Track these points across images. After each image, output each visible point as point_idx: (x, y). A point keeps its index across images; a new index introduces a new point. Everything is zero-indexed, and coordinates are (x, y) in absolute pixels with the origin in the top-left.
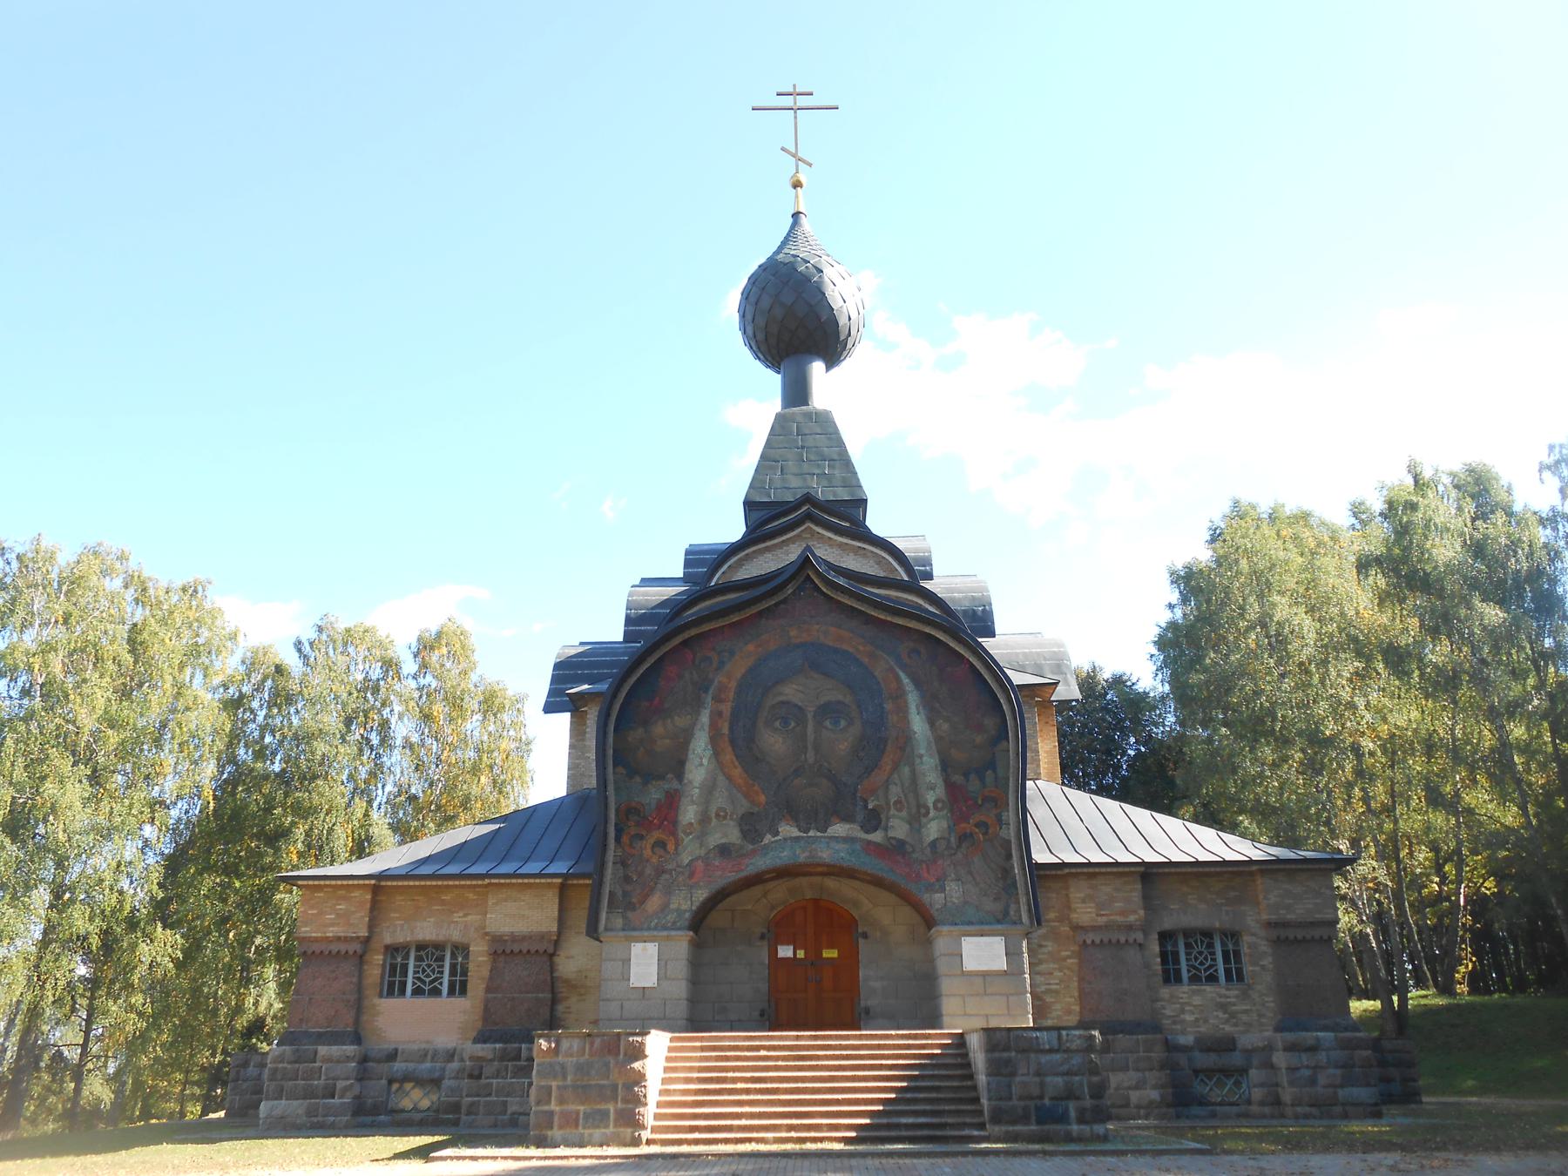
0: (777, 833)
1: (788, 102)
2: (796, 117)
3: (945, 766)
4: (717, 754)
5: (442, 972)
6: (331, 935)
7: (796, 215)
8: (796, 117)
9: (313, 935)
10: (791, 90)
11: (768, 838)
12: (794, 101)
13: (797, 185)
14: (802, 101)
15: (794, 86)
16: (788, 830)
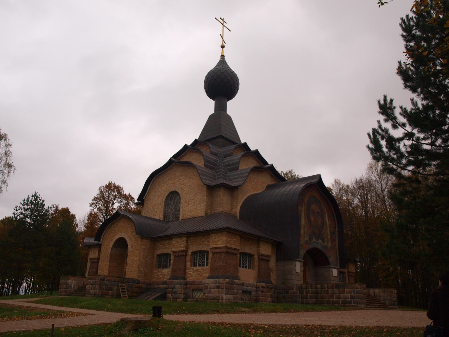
0: (313, 240)
1: (222, 21)
2: (223, 27)
3: (330, 231)
4: (305, 218)
5: (247, 262)
6: (233, 247)
7: (223, 56)
8: (223, 27)
9: (230, 247)
10: (222, 19)
11: (312, 241)
12: (223, 22)
13: (223, 47)
14: (224, 24)
15: (223, 18)
16: (314, 240)
